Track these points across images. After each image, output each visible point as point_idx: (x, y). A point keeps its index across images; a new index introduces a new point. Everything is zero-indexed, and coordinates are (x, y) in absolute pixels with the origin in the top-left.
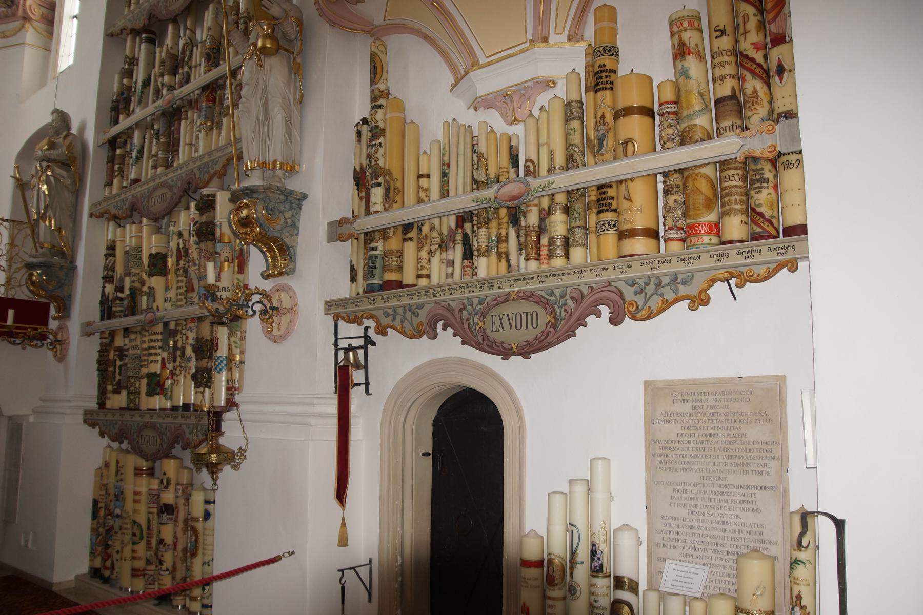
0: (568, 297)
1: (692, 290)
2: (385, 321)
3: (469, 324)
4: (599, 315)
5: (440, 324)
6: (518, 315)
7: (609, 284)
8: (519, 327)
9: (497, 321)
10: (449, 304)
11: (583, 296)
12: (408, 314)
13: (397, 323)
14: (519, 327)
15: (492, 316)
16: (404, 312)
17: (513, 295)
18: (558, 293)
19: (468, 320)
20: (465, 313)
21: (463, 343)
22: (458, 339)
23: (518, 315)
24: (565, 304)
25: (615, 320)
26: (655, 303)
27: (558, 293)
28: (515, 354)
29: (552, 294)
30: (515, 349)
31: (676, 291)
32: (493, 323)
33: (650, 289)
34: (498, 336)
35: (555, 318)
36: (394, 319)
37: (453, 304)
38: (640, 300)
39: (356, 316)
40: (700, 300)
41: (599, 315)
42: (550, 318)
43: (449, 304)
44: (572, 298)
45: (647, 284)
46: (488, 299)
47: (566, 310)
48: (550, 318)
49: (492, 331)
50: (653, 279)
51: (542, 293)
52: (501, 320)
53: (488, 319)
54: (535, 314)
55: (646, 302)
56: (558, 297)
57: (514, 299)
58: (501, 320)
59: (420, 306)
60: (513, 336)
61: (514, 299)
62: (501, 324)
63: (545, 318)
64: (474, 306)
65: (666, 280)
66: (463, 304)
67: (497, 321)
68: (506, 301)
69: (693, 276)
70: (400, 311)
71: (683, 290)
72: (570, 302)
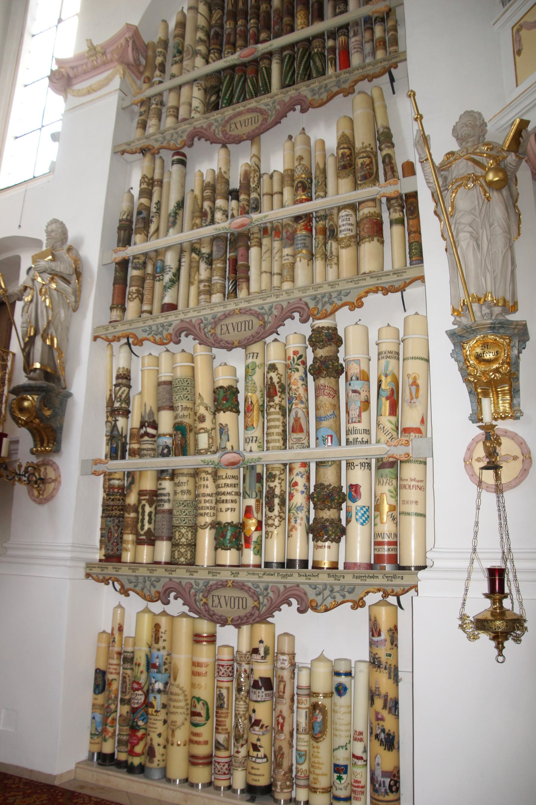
0: (269, 591)
2: (127, 586)
4: (290, 604)
5: (173, 594)
6: (233, 599)
7: (298, 586)
8: (232, 606)
10: (180, 582)
12: (148, 584)
13: (138, 589)
14: (232, 606)
16: (145, 582)
17: (230, 584)
18: (262, 586)
25: (301, 611)
29: (258, 587)
31: (344, 596)
32: (213, 601)
33: (327, 593)
35: (259, 603)
36: (135, 586)
38: (319, 599)
39: (104, 578)
41: (290, 604)
43: (180, 582)
45: (325, 589)
46: (211, 583)
50: (328, 586)
51: (250, 585)
52: (219, 599)
54: (244, 599)
55: (324, 600)
57: (230, 586)
58: (219, 599)
59: (158, 580)
62: (219, 602)
65: (337, 588)
69: (354, 588)
70: (141, 580)
71: (349, 597)
72: (271, 595)
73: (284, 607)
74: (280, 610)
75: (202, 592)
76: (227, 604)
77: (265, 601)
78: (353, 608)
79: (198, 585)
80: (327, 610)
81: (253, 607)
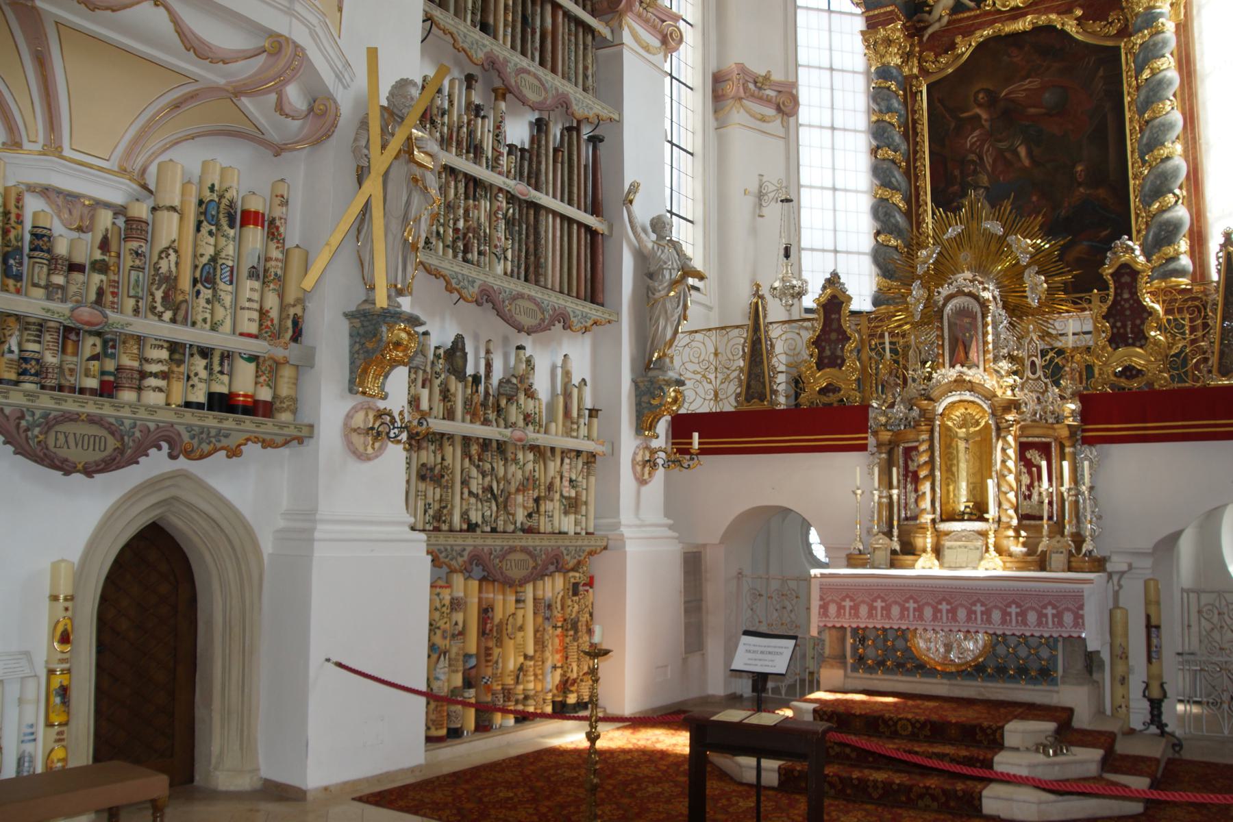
1: (231, 442)
3: (27, 436)
4: (160, 448)
6: (86, 438)
8: (86, 447)
9: (62, 438)
11: (149, 431)
14: (86, 447)
15: (57, 432)
17: (83, 417)
19: (27, 430)
20: (23, 423)
21: (16, 453)
22: (10, 449)
23: (86, 438)
24: (134, 433)
26: (206, 448)
27: (127, 423)
28: (78, 471)
29: (122, 424)
30: (80, 467)
32: (56, 439)
34: (63, 453)
37: (7, 411)
40: (234, 453)
42: (118, 445)
44: (141, 431)
46: (54, 414)
47: (133, 441)
48: (118, 445)
49: (55, 447)
51: (112, 420)
53: (52, 435)
56: (128, 428)
57: (83, 421)
60: (74, 454)
61: (83, 421)
62: (67, 441)
63: (112, 443)
64: (36, 418)
66: (22, 412)
67: (62, 438)
68: (75, 420)
73: (153, 451)
74: (147, 455)
75: (38, 426)
76: (77, 445)
77: (131, 444)
78: (228, 457)
79: (33, 414)
80: (201, 457)
81: (115, 450)
